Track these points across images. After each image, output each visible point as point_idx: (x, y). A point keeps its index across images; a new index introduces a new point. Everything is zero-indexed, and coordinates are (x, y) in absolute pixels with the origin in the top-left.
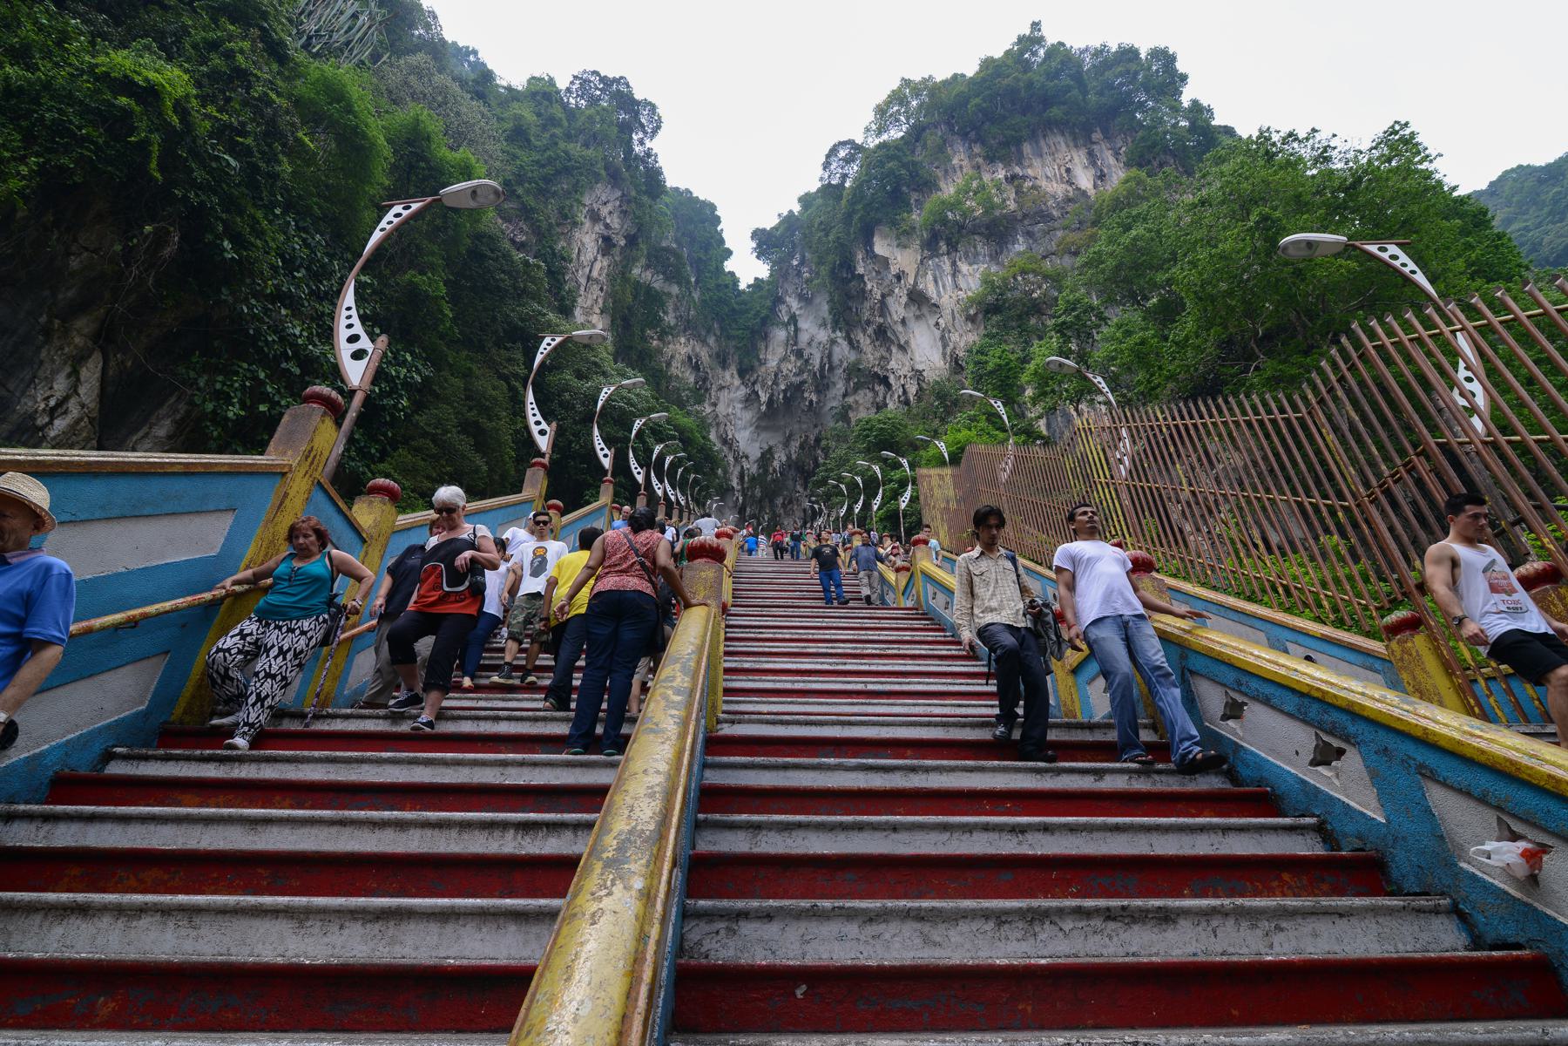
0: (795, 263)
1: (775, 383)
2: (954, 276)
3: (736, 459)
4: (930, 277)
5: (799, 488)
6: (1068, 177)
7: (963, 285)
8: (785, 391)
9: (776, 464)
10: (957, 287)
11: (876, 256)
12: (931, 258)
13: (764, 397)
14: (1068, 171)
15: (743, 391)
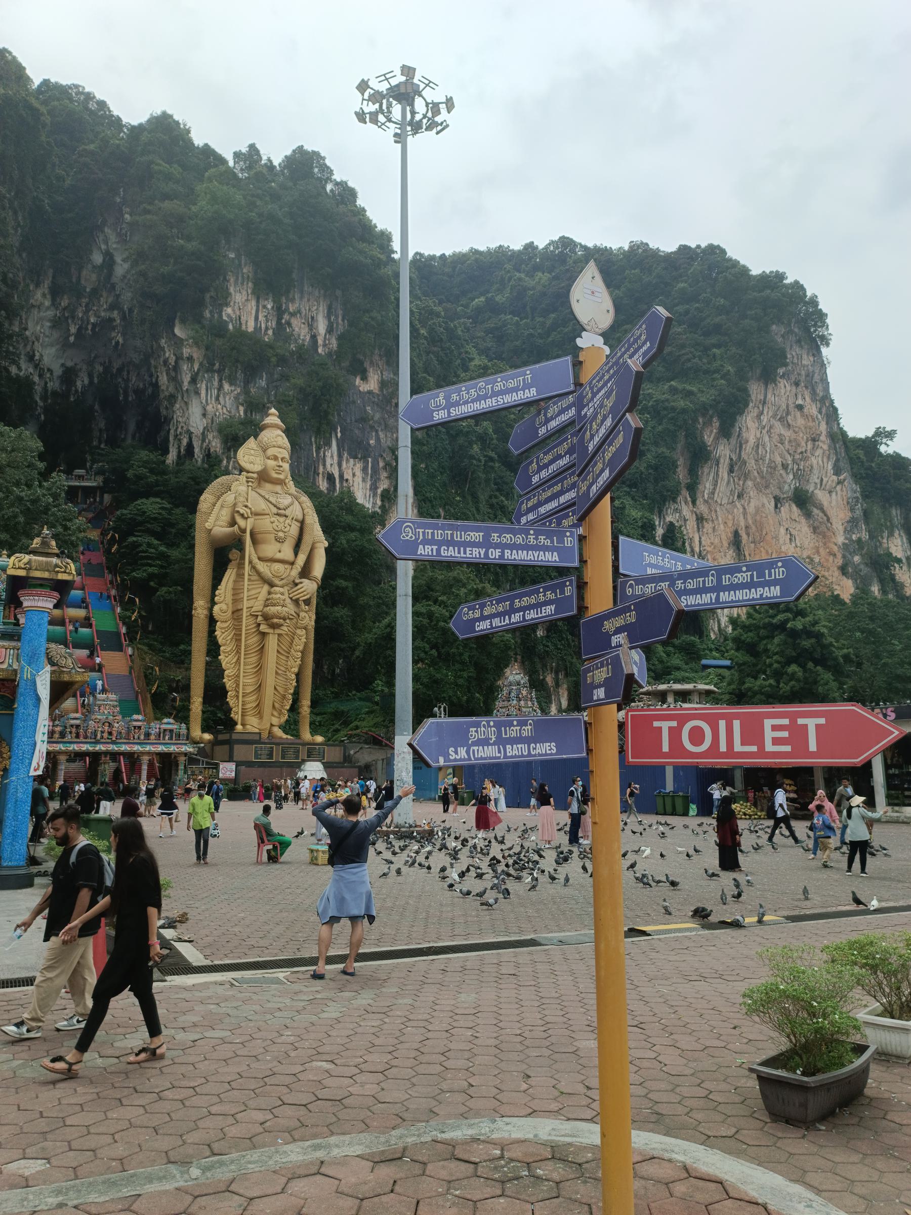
0: (118, 200)
1: (86, 312)
2: (219, 390)
3: (40, 376)
4: (204, 386)
5: (97, 407)
6: (311, 324)
7: (221, 399)
8: (94, 325)
9: (79, 384)
10: (217, 399)
11: (175, 335)
12: (207, 371)
13: (73, 329)
14: (313, 318)
15: (50, 313)
